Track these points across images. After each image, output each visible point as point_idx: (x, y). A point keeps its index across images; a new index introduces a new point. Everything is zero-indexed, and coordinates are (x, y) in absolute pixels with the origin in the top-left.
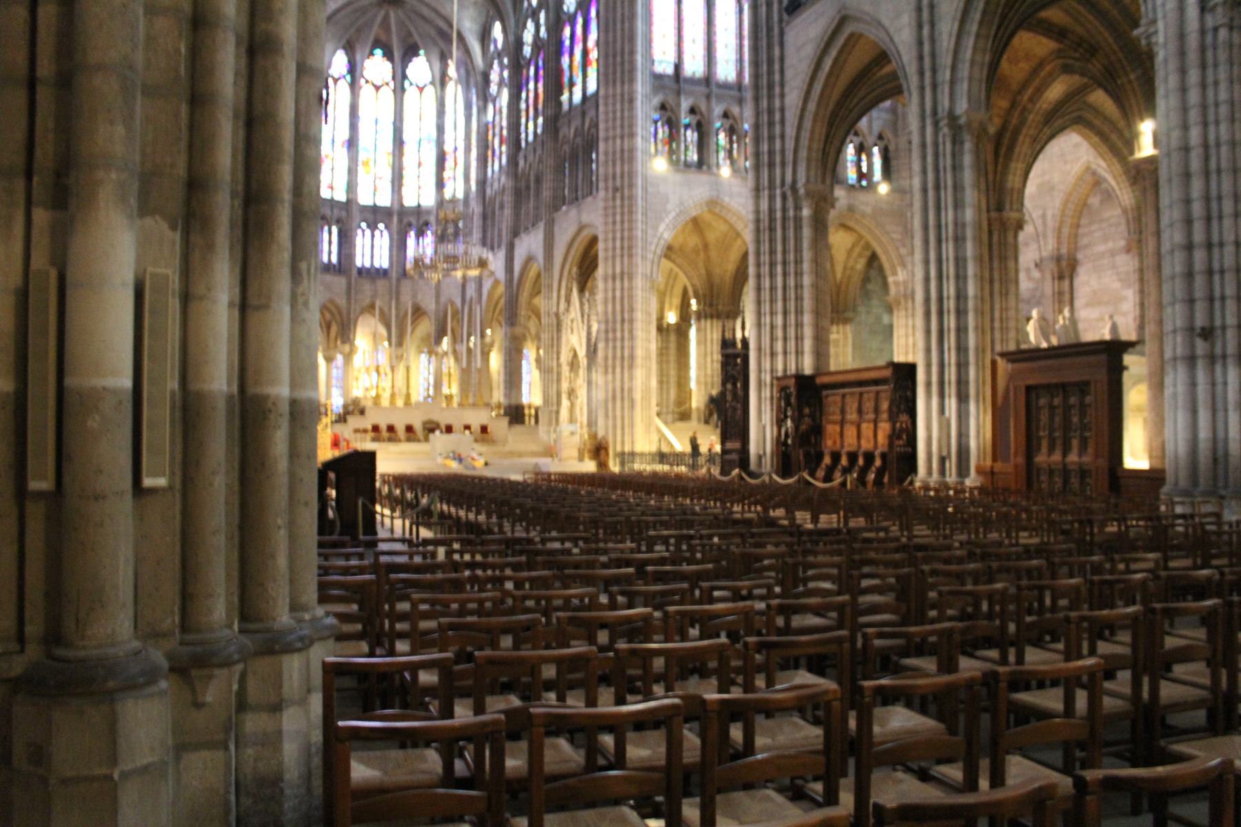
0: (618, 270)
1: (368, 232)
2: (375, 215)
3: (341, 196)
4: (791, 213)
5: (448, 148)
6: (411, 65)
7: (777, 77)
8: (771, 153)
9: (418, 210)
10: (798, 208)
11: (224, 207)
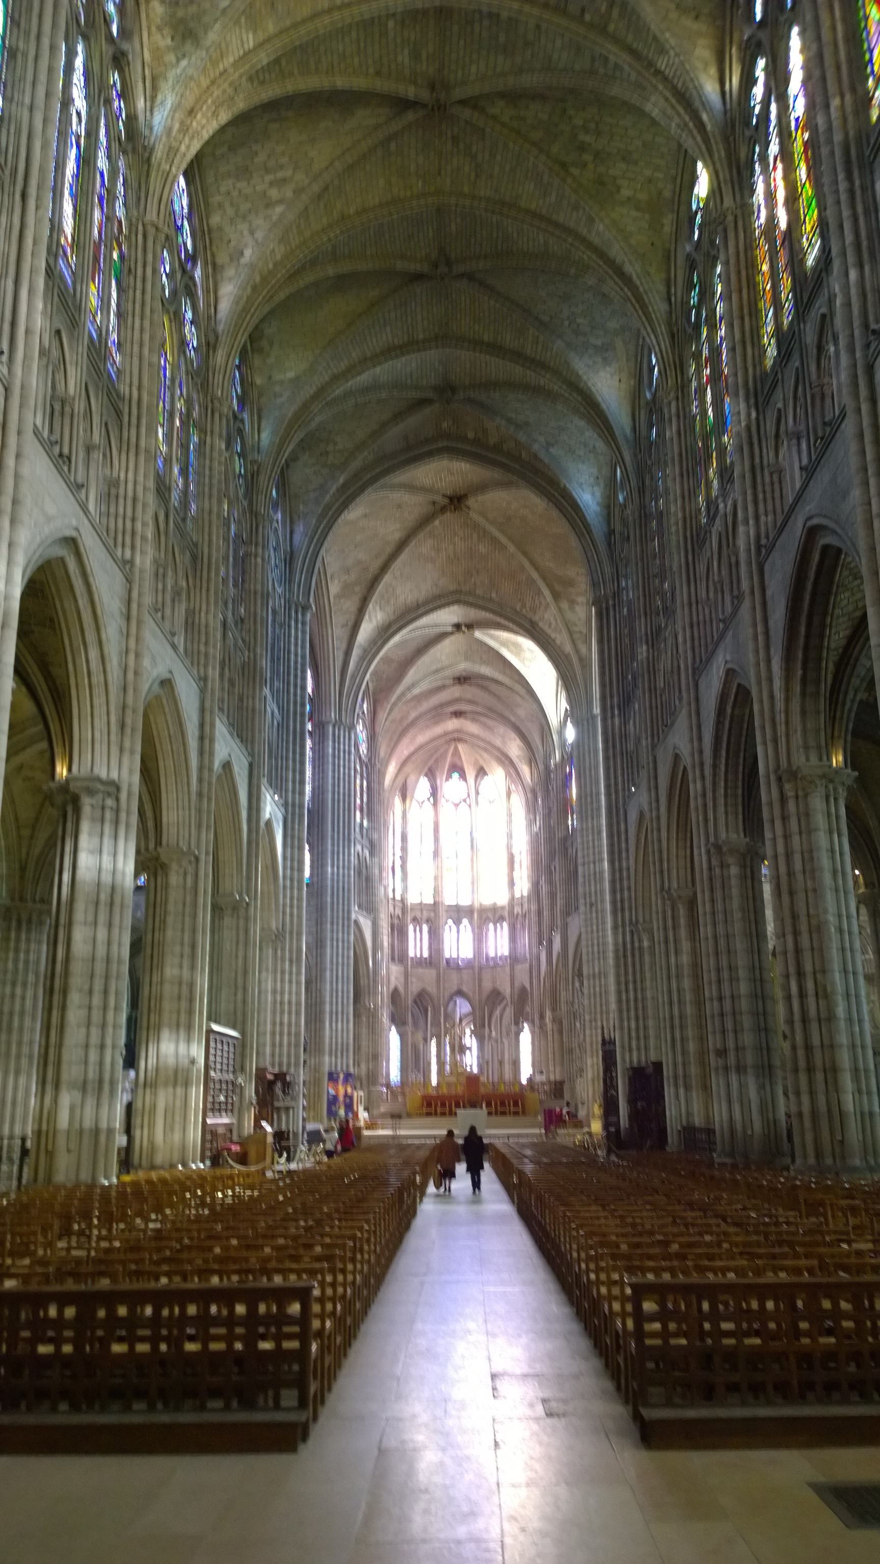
0: (597, 970)
1: (454, 928)
2: (458, 913)
3: (430, 900)
4: (637, 945)
5: (515, 851)
7: (623, 845)
8: (622, 901)
9: (494, 909)
10: (640, 941)
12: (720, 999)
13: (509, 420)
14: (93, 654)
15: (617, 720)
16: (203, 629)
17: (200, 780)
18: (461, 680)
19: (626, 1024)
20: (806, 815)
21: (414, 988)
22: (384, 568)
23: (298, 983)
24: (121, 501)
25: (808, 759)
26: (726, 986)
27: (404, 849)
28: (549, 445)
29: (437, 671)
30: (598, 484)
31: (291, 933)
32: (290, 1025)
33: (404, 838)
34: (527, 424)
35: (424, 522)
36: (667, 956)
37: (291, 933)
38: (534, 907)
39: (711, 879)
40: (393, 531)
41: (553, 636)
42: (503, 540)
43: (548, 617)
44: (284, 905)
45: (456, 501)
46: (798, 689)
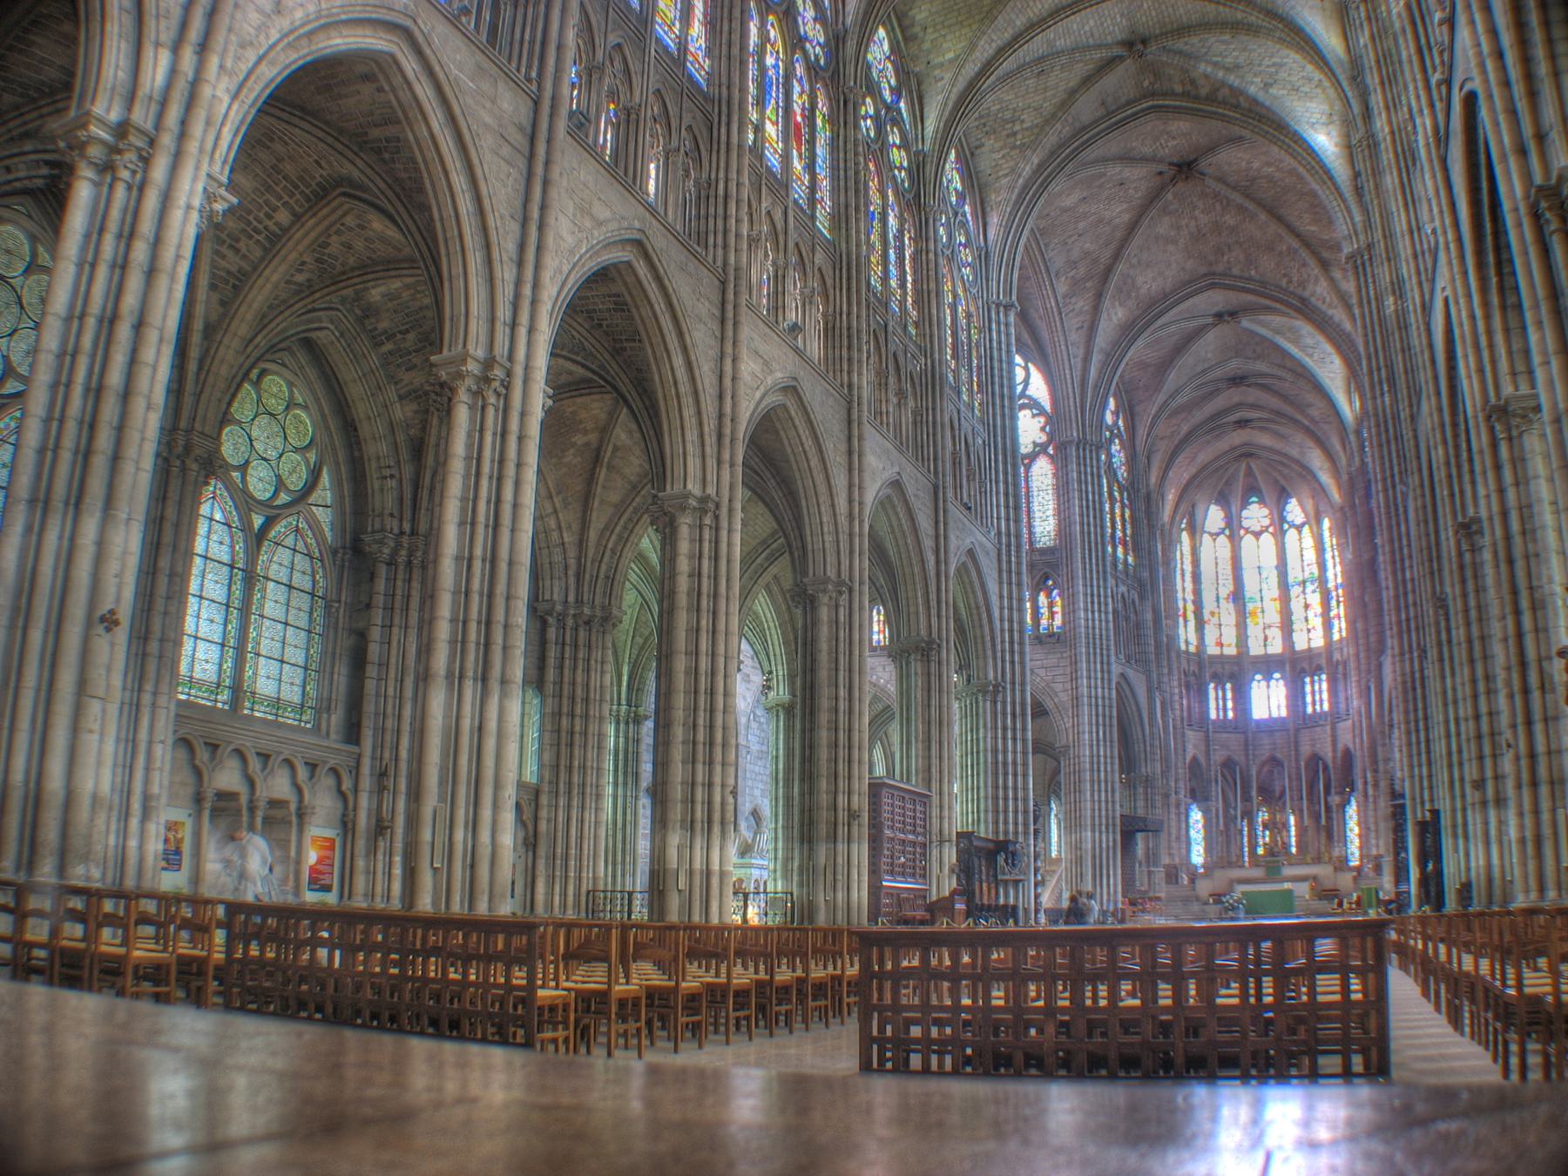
1: (1263, 683)
2: (1268, 665)
3: (1231, 651)
5: (1331, 585)
6: (1289, 507)
7: (1405, 551)
11: (698, 826)
12: (1477, 717)
13: (1216, 64)
14: (678, 361)
15: (1387, 399)
16: (845, 332)
17: (850, 501)
18: (1237, 380)
19: (1416, 770)
20: (1519, 461)
21: (1218, 756)
22: (1117, 256)
23: (1024, 740)
24: (712, 200)
25: (1517, 389)
26: (1482, 700)
27: (1197, 592)
28: (1267, 86)
29: (1204, 372)
30: (1332, 123)
31: (1013, 683)
32: (1015, 789)
33: (1196, 577)
34: (1237, 67)
35: (1153, 197)
36: (1443, 678)
37: (1013, 683)
38: (1352, 651)
39: (1462, 567)
40: (1119, 213)
41: (1330, 312)
42: (1251, 206)
43: (1320, 291)
44: (1003, 651)
45: (1185, 168)
46: (1495, 300)
